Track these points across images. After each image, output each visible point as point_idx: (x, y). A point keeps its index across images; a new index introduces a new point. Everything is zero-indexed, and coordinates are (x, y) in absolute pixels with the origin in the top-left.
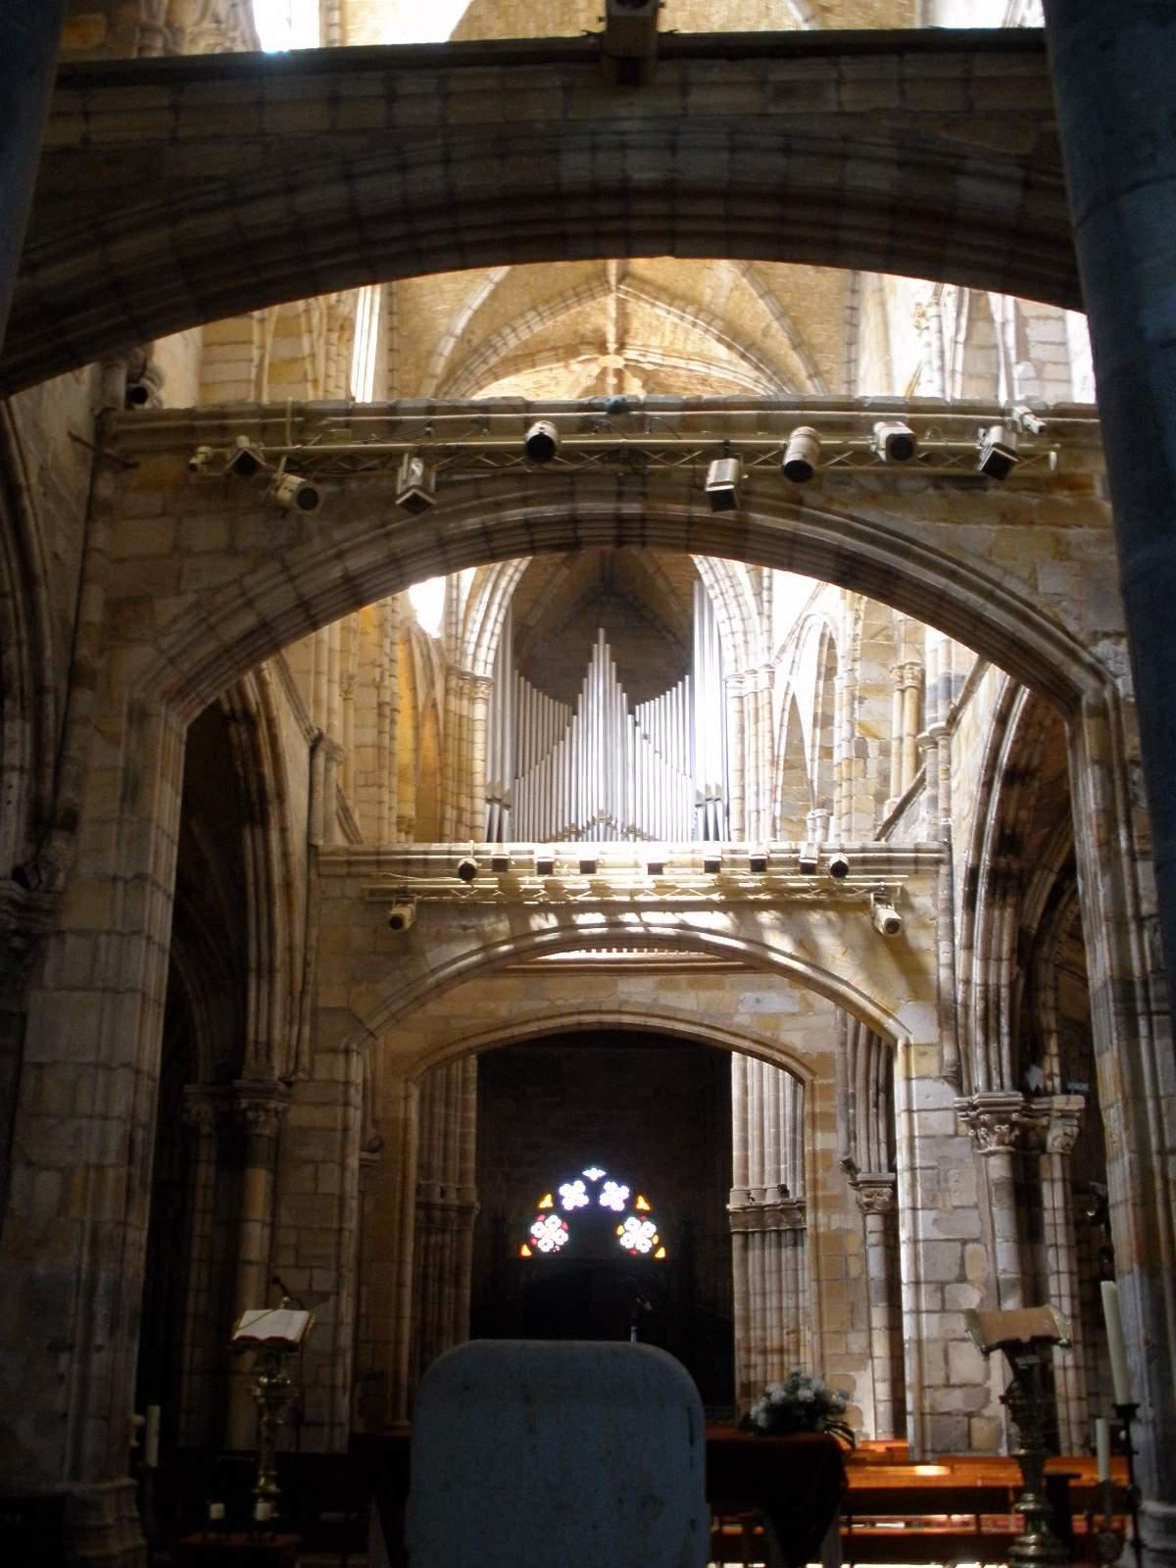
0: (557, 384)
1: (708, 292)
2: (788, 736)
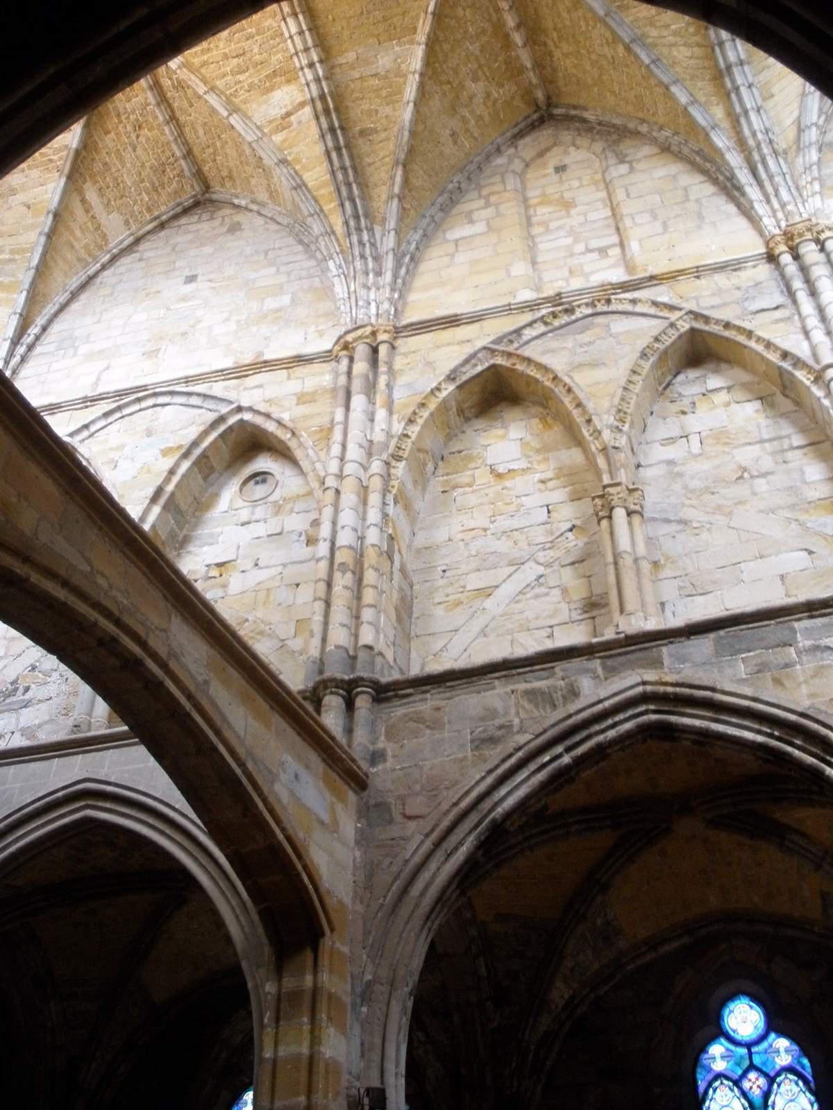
1: (351, 56)
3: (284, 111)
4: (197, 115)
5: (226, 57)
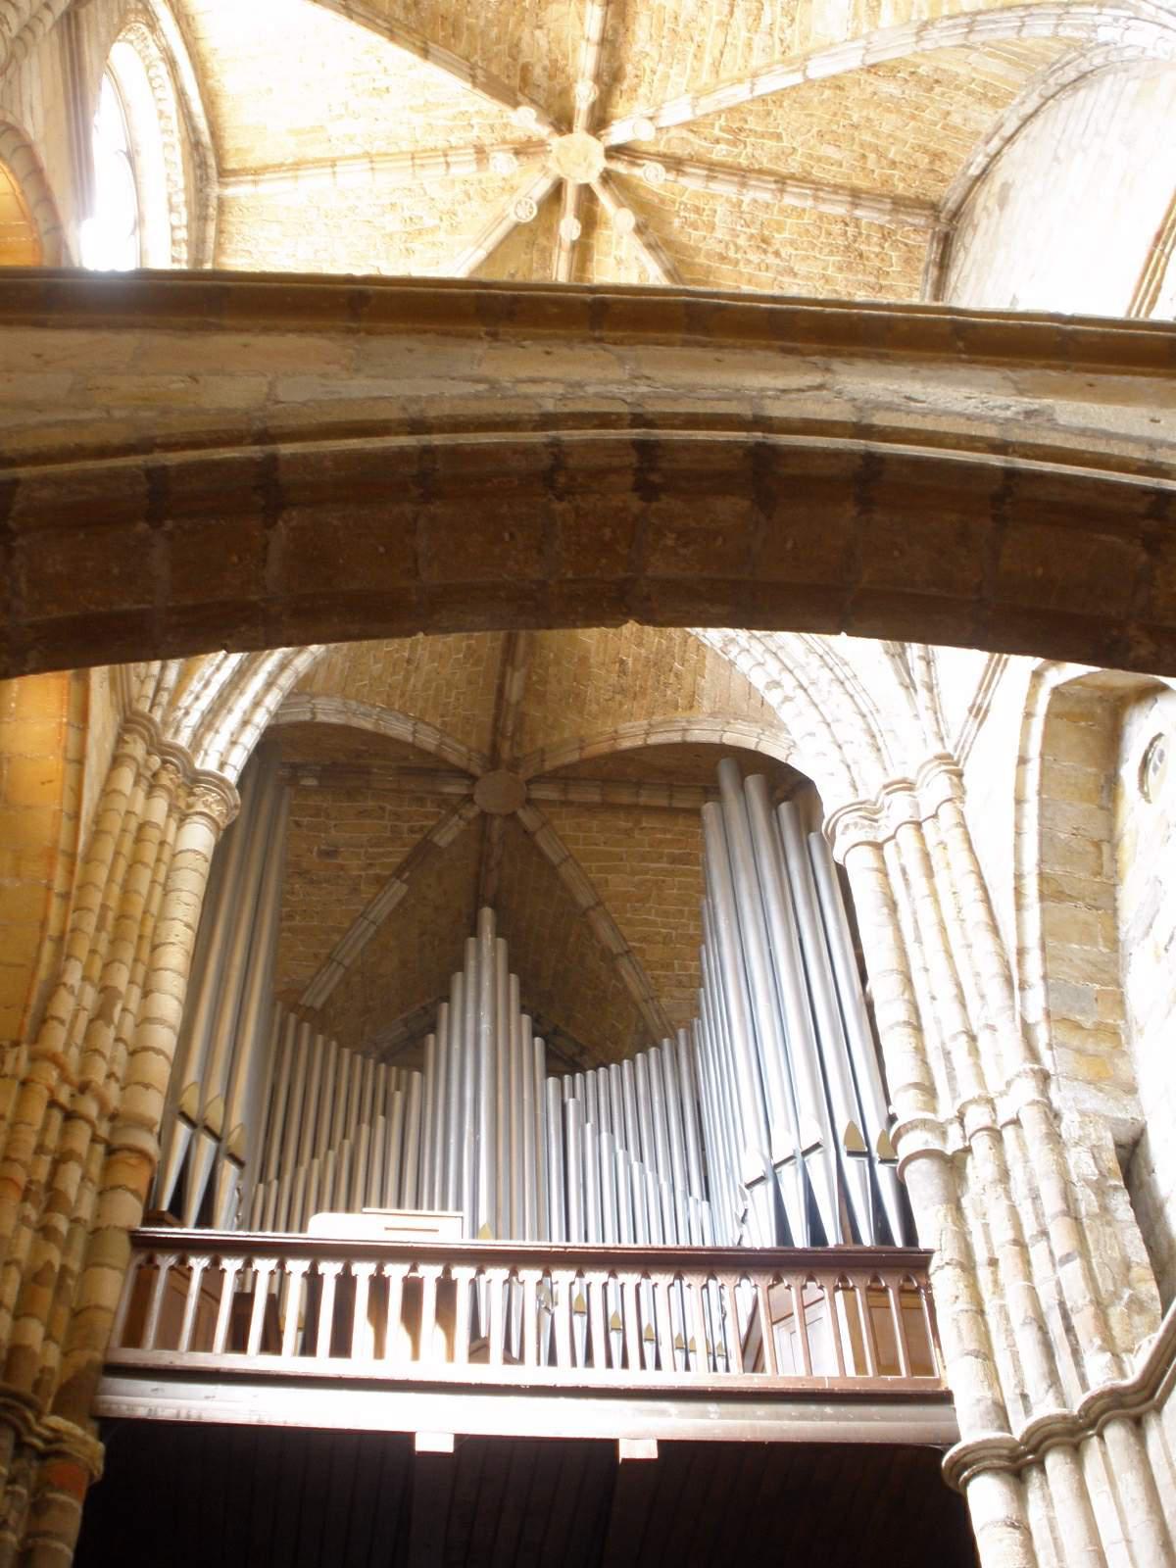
2: (1041, 816)
4: (800, 139)
5: (724, 25)
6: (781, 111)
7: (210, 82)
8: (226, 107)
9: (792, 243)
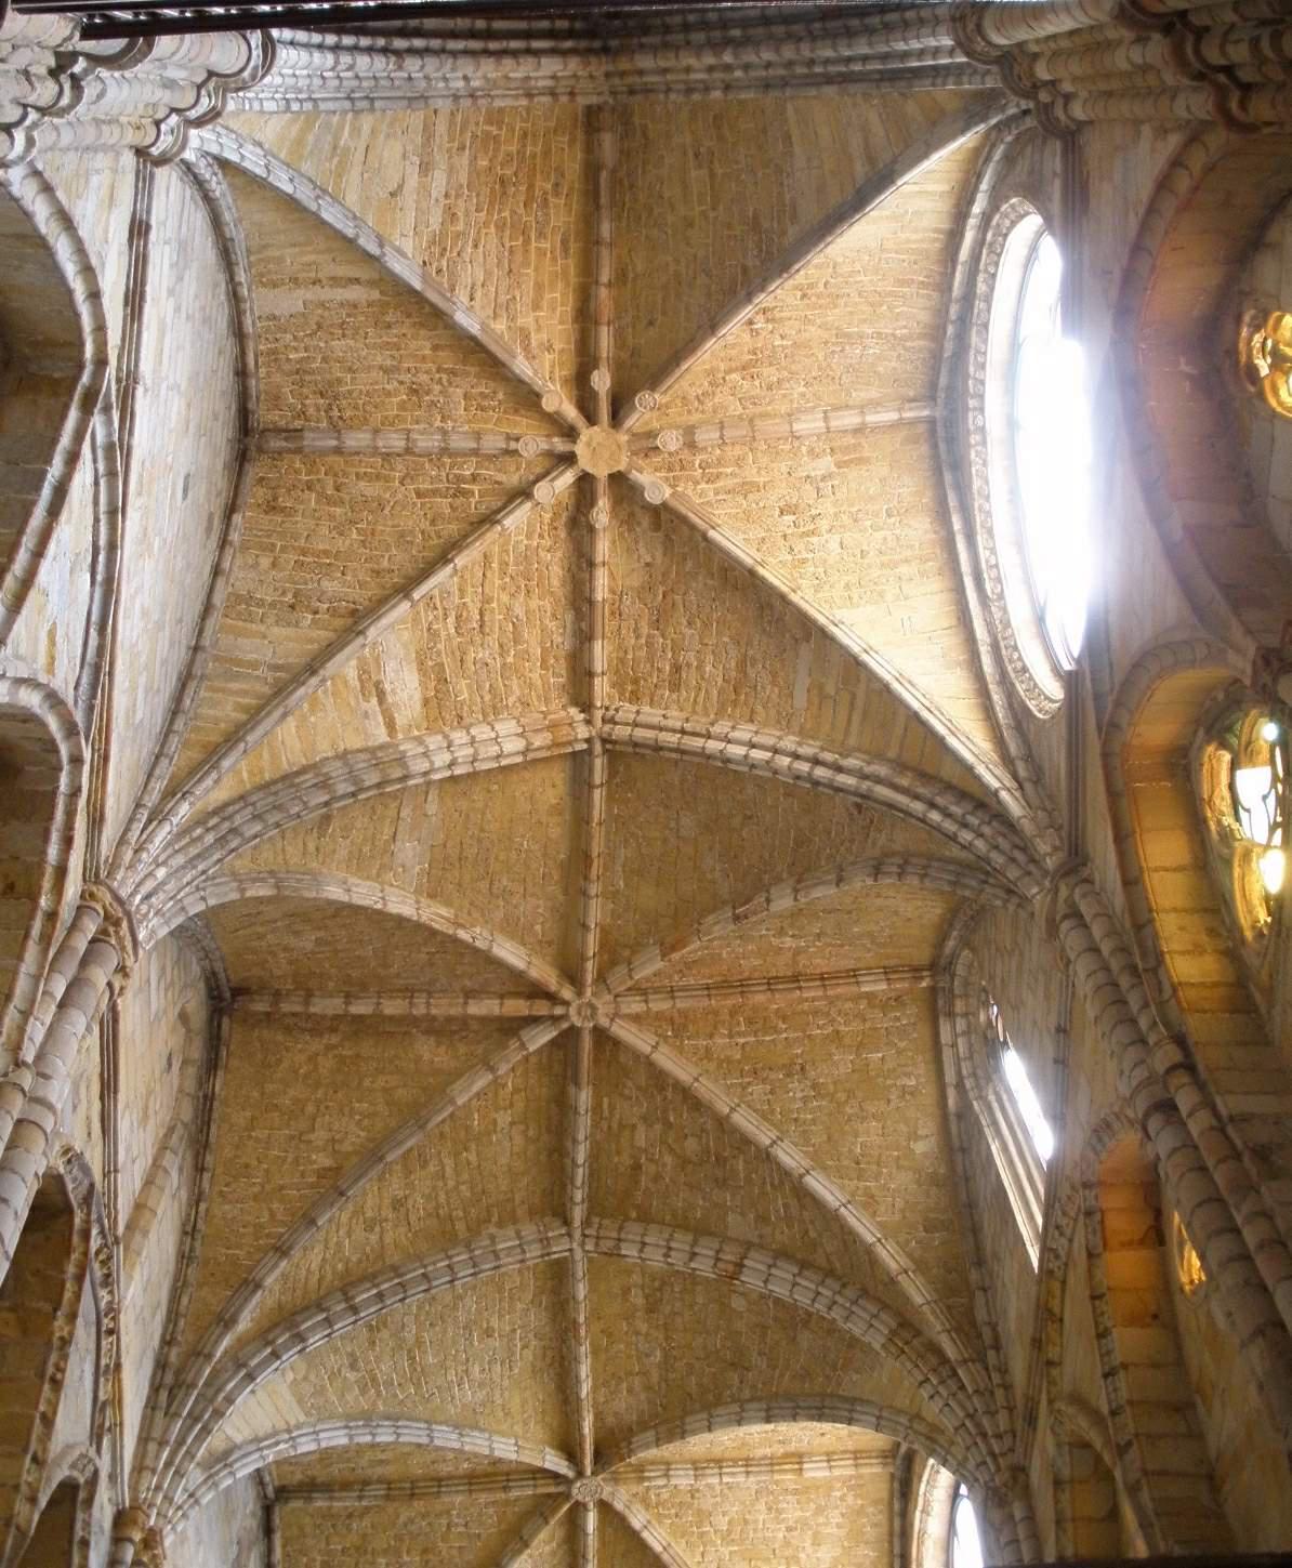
0: (711, 372)
1: (432, 807)
3: (387, 687)
5: (487, 600)
6: (422, 526)
7: (943, 533)
8: (927, 499)
9: (389, 394)
